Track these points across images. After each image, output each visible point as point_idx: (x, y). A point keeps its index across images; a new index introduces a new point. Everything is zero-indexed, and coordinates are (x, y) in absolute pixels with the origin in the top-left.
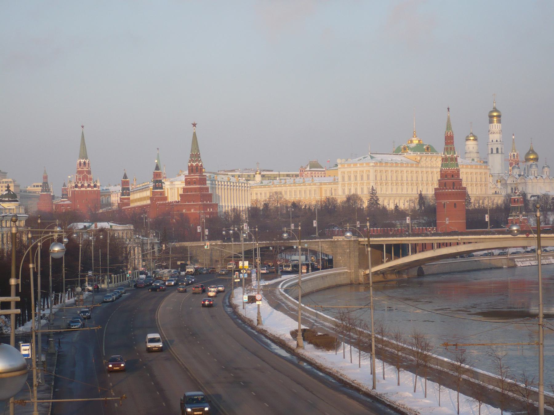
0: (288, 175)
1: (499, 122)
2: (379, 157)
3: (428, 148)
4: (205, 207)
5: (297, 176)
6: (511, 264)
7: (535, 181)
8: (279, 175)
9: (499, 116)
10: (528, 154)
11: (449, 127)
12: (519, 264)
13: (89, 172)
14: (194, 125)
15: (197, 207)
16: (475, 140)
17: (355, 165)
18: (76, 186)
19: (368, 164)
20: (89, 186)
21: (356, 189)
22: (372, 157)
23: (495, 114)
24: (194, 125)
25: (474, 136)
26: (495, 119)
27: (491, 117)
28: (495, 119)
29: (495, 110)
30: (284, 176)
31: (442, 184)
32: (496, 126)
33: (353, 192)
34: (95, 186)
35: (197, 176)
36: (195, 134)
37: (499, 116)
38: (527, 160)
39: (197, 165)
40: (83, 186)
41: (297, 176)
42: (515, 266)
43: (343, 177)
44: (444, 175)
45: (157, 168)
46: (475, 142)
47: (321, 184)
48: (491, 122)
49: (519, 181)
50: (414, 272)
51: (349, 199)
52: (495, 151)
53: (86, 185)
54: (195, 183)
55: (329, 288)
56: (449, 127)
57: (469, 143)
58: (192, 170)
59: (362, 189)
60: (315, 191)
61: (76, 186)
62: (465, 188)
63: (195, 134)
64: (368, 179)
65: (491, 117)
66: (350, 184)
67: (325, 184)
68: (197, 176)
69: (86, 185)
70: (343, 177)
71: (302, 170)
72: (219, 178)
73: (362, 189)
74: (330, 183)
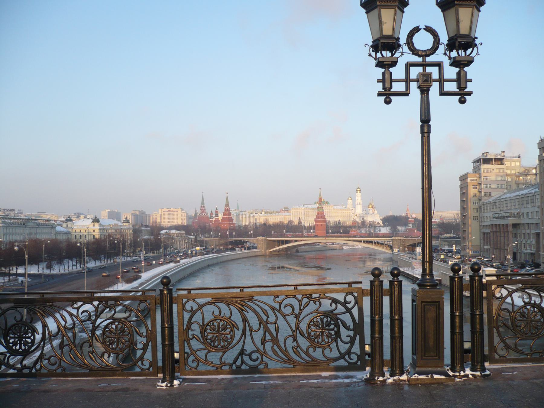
0: (277, 212)
1: (360, 192)
2: (306, 206)
3: (326, 203)
4: (230, 224)
5: (280, 212)
6: (341, 248)
7: (371, 215)
8: (274, 212)
9: (360, 190)
10: (369, 205)
11: (320, 195)
12: (344, 248)
13: (205, 210)
14: (227, 193)
15: (227, 224)
16: (351, 199)
17: (297, 208)
18: (200, 215)
19: (302, 208)
20: (205, 215)
21: (293, 218)
22: (303, 206)
23: (358, 190)
24: (227, 193)
25: (351, 198)
26: (358, 191)
27: (357, 191)
28: (358, 191)
29: (359, 188)
30: (275, 212)
31: (317, 217)
32: (359, 194)
33: (292, 219)
34: (207, 215)
35: (227, 213)
36: (227, 197)
37: (360, 190)
38: (369, 207)
39: (228, 209)
40: (202, 215)
41: (280, 212)
42: (343, 249)
43: (293, 213)
44: (318, 214)
45: (217, 209)
46: (351, 200)
47: (285, 216)
48: (357, 193)
49: (365, 215)
50: (294, 250)
51: (289, 222)
52: (358, 204)
53: (203, 214)
54: (227, 215)
55: (251, 257)
56: (320, 195)
57: (349, 200)
58: (226, 210)
59: (295, 218)
60: (283, 218)
61: (200, 215)
62: (326, 219)
63: (227, 197)
64: (302, 214)
65: (357, 191)
66: (295, 216)
67: (287, 216)
68: (227, 213)
69: (203, 214)
70: (293, 213)
71: (281, 210)
72: (241, 213)
73: (295, 218)
74: (288, 215)
